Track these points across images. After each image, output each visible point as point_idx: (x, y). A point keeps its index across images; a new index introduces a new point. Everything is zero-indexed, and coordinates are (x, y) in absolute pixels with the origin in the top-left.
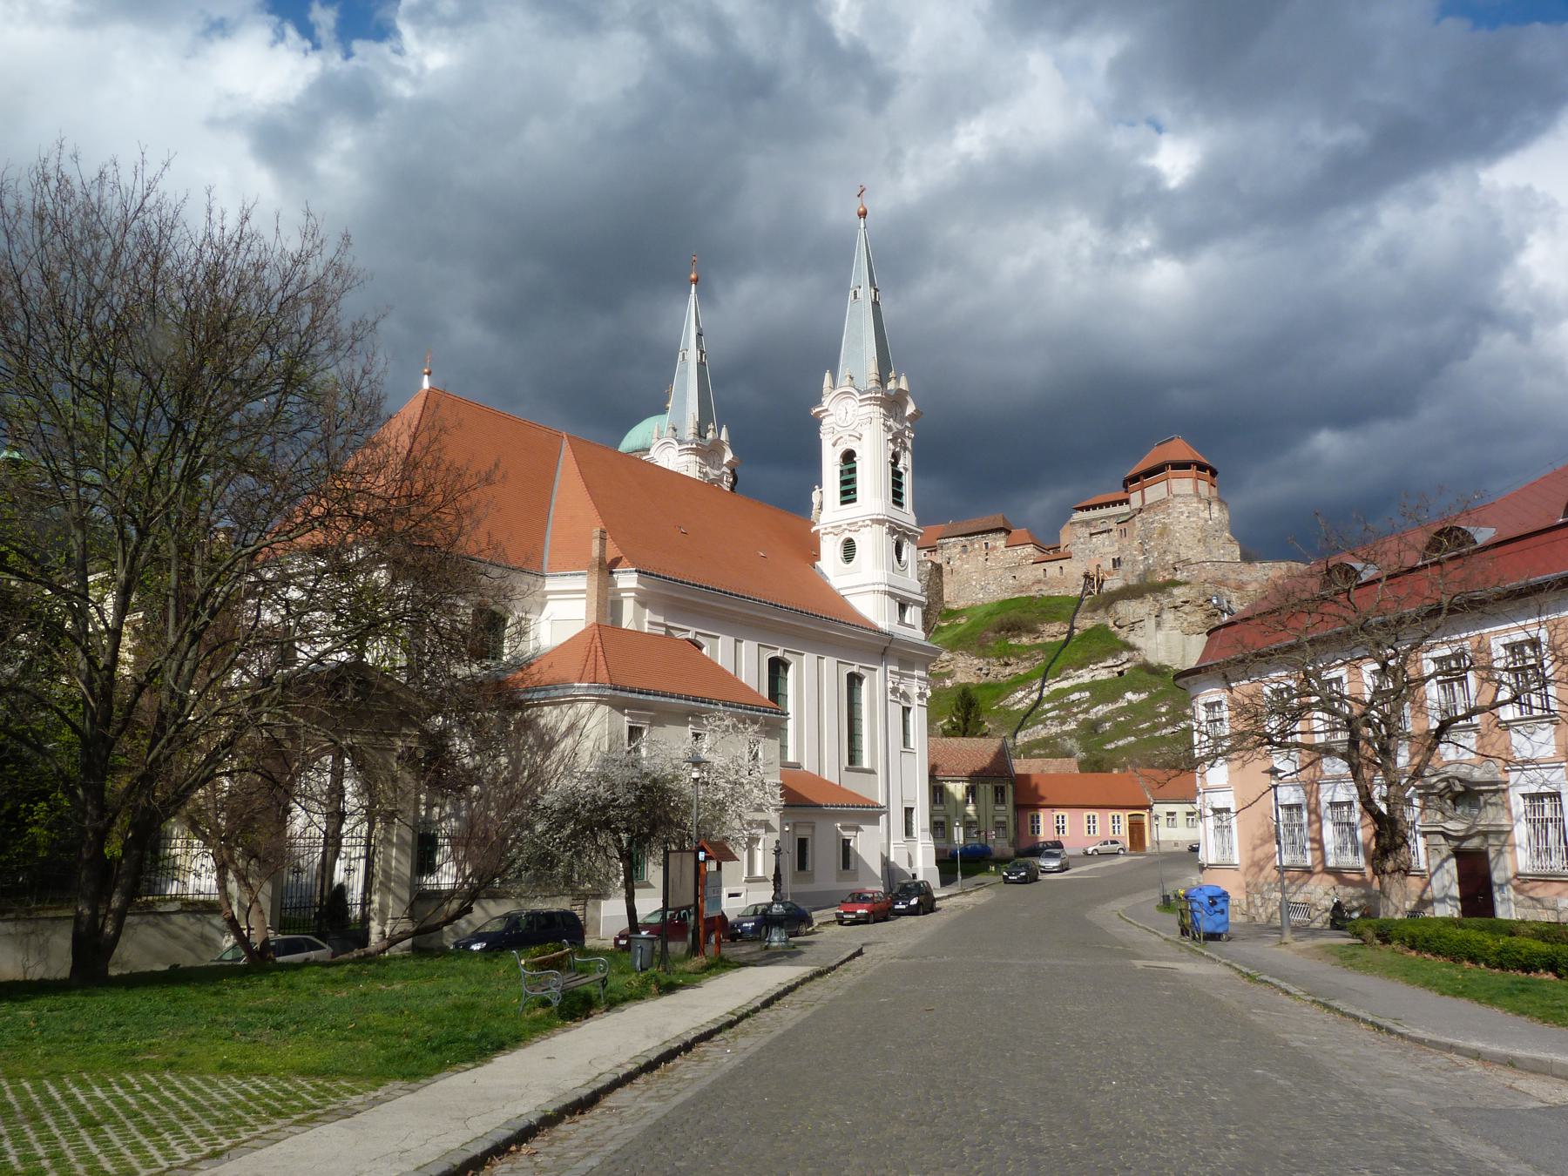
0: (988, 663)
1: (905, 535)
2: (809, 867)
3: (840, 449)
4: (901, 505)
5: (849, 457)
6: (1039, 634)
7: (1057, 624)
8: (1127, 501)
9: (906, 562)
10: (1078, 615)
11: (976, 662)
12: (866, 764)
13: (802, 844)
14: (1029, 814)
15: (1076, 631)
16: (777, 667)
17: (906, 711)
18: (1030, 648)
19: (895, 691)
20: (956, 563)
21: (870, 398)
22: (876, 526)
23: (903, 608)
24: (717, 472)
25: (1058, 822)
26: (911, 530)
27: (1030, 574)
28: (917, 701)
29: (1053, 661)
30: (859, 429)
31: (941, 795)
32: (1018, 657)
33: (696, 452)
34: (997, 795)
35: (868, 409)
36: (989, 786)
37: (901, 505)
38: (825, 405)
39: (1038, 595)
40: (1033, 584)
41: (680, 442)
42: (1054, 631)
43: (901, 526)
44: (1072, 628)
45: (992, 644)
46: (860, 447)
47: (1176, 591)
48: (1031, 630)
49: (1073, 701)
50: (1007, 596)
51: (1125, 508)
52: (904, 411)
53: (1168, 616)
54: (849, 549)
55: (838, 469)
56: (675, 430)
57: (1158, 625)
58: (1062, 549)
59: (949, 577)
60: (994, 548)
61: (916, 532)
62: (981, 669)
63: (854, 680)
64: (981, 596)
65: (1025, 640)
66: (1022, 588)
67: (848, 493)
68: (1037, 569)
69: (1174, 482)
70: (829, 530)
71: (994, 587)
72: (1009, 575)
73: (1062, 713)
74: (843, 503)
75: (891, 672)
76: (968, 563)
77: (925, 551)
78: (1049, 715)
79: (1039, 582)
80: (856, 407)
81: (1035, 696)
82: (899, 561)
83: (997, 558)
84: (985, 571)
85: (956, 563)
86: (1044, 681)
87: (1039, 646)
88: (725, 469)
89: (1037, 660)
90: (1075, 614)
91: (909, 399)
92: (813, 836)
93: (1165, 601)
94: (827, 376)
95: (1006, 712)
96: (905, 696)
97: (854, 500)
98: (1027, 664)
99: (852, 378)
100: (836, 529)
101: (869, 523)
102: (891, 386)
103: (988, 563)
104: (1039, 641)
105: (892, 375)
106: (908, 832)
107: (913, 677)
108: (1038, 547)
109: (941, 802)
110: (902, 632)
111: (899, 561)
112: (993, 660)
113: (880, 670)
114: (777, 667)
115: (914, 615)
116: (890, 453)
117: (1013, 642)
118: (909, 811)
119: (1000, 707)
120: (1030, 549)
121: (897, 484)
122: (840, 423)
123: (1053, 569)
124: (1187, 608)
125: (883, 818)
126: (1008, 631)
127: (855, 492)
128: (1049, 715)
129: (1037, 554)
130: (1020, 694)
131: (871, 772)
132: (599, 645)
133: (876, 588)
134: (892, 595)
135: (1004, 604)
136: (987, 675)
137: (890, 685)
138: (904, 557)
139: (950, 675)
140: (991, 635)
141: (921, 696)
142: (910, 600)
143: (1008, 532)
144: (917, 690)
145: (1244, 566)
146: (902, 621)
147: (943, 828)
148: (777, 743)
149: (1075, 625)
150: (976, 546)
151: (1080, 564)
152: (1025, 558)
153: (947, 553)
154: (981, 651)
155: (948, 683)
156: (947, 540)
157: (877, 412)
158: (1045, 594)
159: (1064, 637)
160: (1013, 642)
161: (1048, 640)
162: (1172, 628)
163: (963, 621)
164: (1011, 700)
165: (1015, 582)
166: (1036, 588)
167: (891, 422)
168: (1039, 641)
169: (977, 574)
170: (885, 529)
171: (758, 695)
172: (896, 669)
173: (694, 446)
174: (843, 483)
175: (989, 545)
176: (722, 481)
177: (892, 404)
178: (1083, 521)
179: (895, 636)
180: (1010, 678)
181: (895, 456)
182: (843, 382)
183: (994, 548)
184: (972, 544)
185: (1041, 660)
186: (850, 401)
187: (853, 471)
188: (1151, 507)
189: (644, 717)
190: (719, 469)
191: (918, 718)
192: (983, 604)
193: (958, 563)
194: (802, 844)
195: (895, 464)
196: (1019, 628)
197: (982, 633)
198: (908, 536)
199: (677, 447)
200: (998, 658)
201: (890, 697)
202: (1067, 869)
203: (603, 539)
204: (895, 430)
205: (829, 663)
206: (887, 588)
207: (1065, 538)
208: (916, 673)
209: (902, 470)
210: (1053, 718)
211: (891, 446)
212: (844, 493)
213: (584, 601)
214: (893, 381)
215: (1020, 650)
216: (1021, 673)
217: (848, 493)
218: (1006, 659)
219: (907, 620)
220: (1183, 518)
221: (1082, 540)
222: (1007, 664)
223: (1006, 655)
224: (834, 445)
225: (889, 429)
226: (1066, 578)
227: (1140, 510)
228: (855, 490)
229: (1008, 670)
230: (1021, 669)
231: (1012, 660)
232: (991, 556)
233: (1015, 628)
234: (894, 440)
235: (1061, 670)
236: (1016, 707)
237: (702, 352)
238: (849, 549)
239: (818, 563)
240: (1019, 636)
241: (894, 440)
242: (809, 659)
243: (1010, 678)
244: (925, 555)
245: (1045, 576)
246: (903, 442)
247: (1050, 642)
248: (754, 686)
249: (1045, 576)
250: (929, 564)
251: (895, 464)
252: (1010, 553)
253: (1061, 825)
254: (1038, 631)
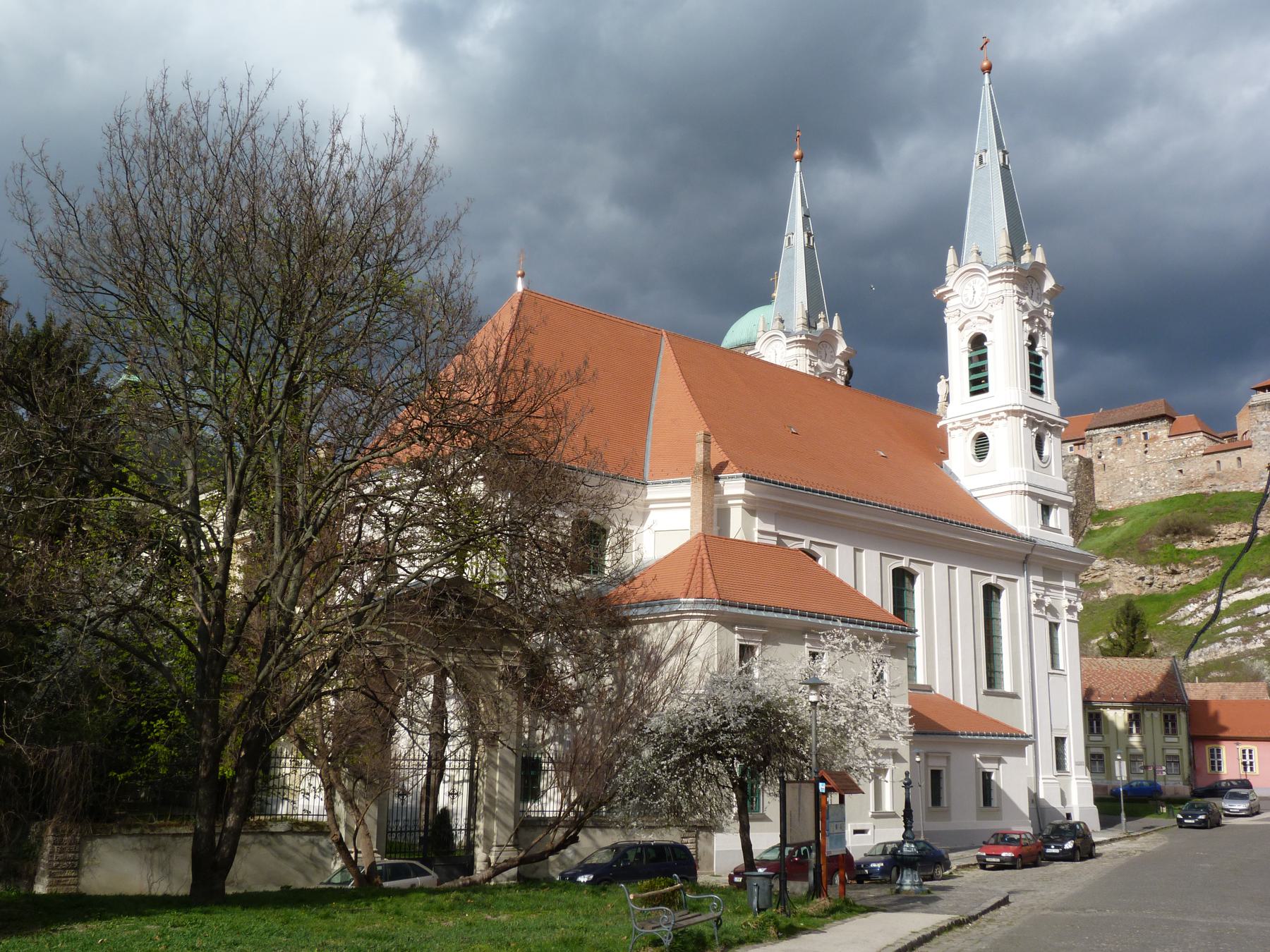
0: (1151, 571)
1: (1047, 427)
2: (944, 802)
4: (1040, 393)
5: (978, 342)
6: (1214, 536)
7: (1236, 524)
9: (1049, 458)
10: (1262, 514)
11: (1136, 570)
12: (1007, 687)
13: (936, 776)
14: (1208, 747)
15: (1261, 533)
16: (902, 579)
17: (1054, 627)
18: (1202, 553)
19: (1039, 604)
21: (1001, 275)
22: (1013, 418)
23: (1046, 509)
24: (829, 365)
25: (1244, 757)
26: (1054, 422)
27: (1199, 468)
28: (1066, 616)
29: (1233, 567)
30: (990, 311)
31: (1098, 724)
32: (1188, 563)
33: (806, 344)
34: (1166, 725)
35: (999, 287)
36: (1156, 714)
37: (1040, 393)
38: (950, 285)
39: (1211, 491)
40: (1205, 478)
41: (788, 334)
42: (1232, 533)
43: (1042, 418)
44: (1255, 529)
45: (1155, 549)
46: (991, 330)
48: (1203, 533)
49: (1259, 615)
50: (1172, 493)
52: (1041, 286)
54: (982, 444)
55: (966, 356)
56: (782, 321)
58: (1239, 437)
59: (1101, 473)
60: (1155, 438)
61: (1060, 423)
62: (1142, 579)
63: (991, 593)
64: (1140, 494)
65: (1197, 544)
66: (1191, 484)
67: (979, 383)
68: (1209, 461)
70: (958, 424)
71: (1156, 483)
72: (1173, 469)
73: (1246, 629)
74: (973, 393)
75: (1035, 583)
76: (1123, 457)
77: (1071, 445)
78: (1230, 631)
79: (1212, 476)
80: (985, 286)
81: (1211, 609)
82: (1040, 456)
83: (1160, 449)
84: (1145, 465)
85: (1108, 457)
86: (1221, 591)
87: (1214, 550)
88: (838, 362)
89: (1212, 567)
90: (1258, 512)
91: (1047, 273)
92: (948, 767)
94: (951, 254)
95: (1176, 627)
96: (1051, 610)
97: (986, 390)
98: (1199, 572)
99: (979, 253)
100: (966, 423)
101: (1004, 415)
102: (1025, 259)
103: (1148, 456)
104: (1214, 545)
105: (1026, 246)
106: (1060, 765)
107: (1060, 588)
108: (1210, 435)
109: (1099, 731)
110: (1046, 537)
111: (1040, 456)
112: (1157, 568)
113: (1022, 581)
114: (902, 579)
115: (1059, 518)
116: (1026, 336)
117: (1181, 546)
118: (1060, 741)
119: (1170, 622)
120: (1199, 438)
122: (967, 304)
123: (1229, 460)
125: (1029, 749)
126: (1176, 533)
127: (987, 381)
128: (1230, 631)
129: (1209, 443)
130: (1192, 607)
131: (1014, 696)
132: (705, 556)
133: (1014, 488)
134: (1033, 495)
135: (1170, 501)
136: (1151, 585)
137: (1034, 597)
138: (1046, 453)
139: (1105, 585)
140: (1154, 538)
141: (1071, 609)
142: (1054, 500)
143: (1172, 419)
144: (1065, 603)
146: (1045, 525)
147: (1102, 762)
148: (905, 663)
149: (1258, 526)
150: (1133, 437)
151: (1263, 454)
152: (1194, 449)
153: (1097, 446)
154: (1143, 558)
155: (1104, 595)
156: (1097, 431)
157: (1010, 289)
158: (1220, 490)
159: (1245, 540)
160: (1181, 546)
161: (1225, 543)
163: (1119, 523)
164: (1181, 614)
165: (1182, 477)
166: (1208, 483)
167: (1026, 300)
168: (1214, 545)
169: (1134, 469)
170: (1022, 422)
171: (881, 609)
172: (1040, 579)
173: (804, 338)
174: (973, 371)
175: (1149, 436)
176: (834, 374)
177: (1027, 280)
178: (1266, 403)
179: (1039, 542)
180: (1179, 588)
181: (1033, 339)
182: (969, 258)
183: (1155, 438)
184: (1128, 435)
185: (1217, 567)
186: (978, 279)
187: (983, 357)
189: (756, 634)
190: (831, 361)
191: (1068, 636)
192: (1144, 504)
193: (1111, 457)
194: (936, 776)
195: (1032, 347)
196: (1189, 531)
197: (1143, 537)
198: (1050, 429)
199: (785, 340)
200: (1164, 565)
201: (1034, 611)
202: (1258, 813)
203: (707, 442)
204: (1031, 309)
205: (962, 573)
206: (1027, 488)
207: (1242, 424)
208: (1064, 583)
209: (1041, 354)
210: (1234, 635)
211: (1027, 327)
212: (974, 383)
213: (688, 511)
214: (1027, 254)
215: (1190, 556)
216: (1193, 583)
217: (979, 383)
218: (1173, 567)
219: (1052, 523)
221: (1264, 425)
222: (1174, 573)
223: (1173, 562)
224: (961, 329)
225: (1025, 308)
226: (1245, 471)
228: (986, 379)
229: (1176, 579)
230: (1193, 577)
231: (1181, 567)
232: (1151, 448)
233: (1183, 530)
234: (1030, 321)
235: (1244, 577)
236: (1188, 622)
237: (809, 235)
238: (982, 444)
239: (945, 462)
240: (1189, 539)
241: (1030, 321)
242: (938, 570)
243: (1179, 588)
244: (1071, 449)
245: (1219, 468)
246: (1041, 322)
247: (1228, 547)
248: (877, 600)
249: (1219, 468)
250: (1077, 460)
251: (1032, 347)
252: (1174, 443)
253: (1248, 760)
254: (1212, 534)
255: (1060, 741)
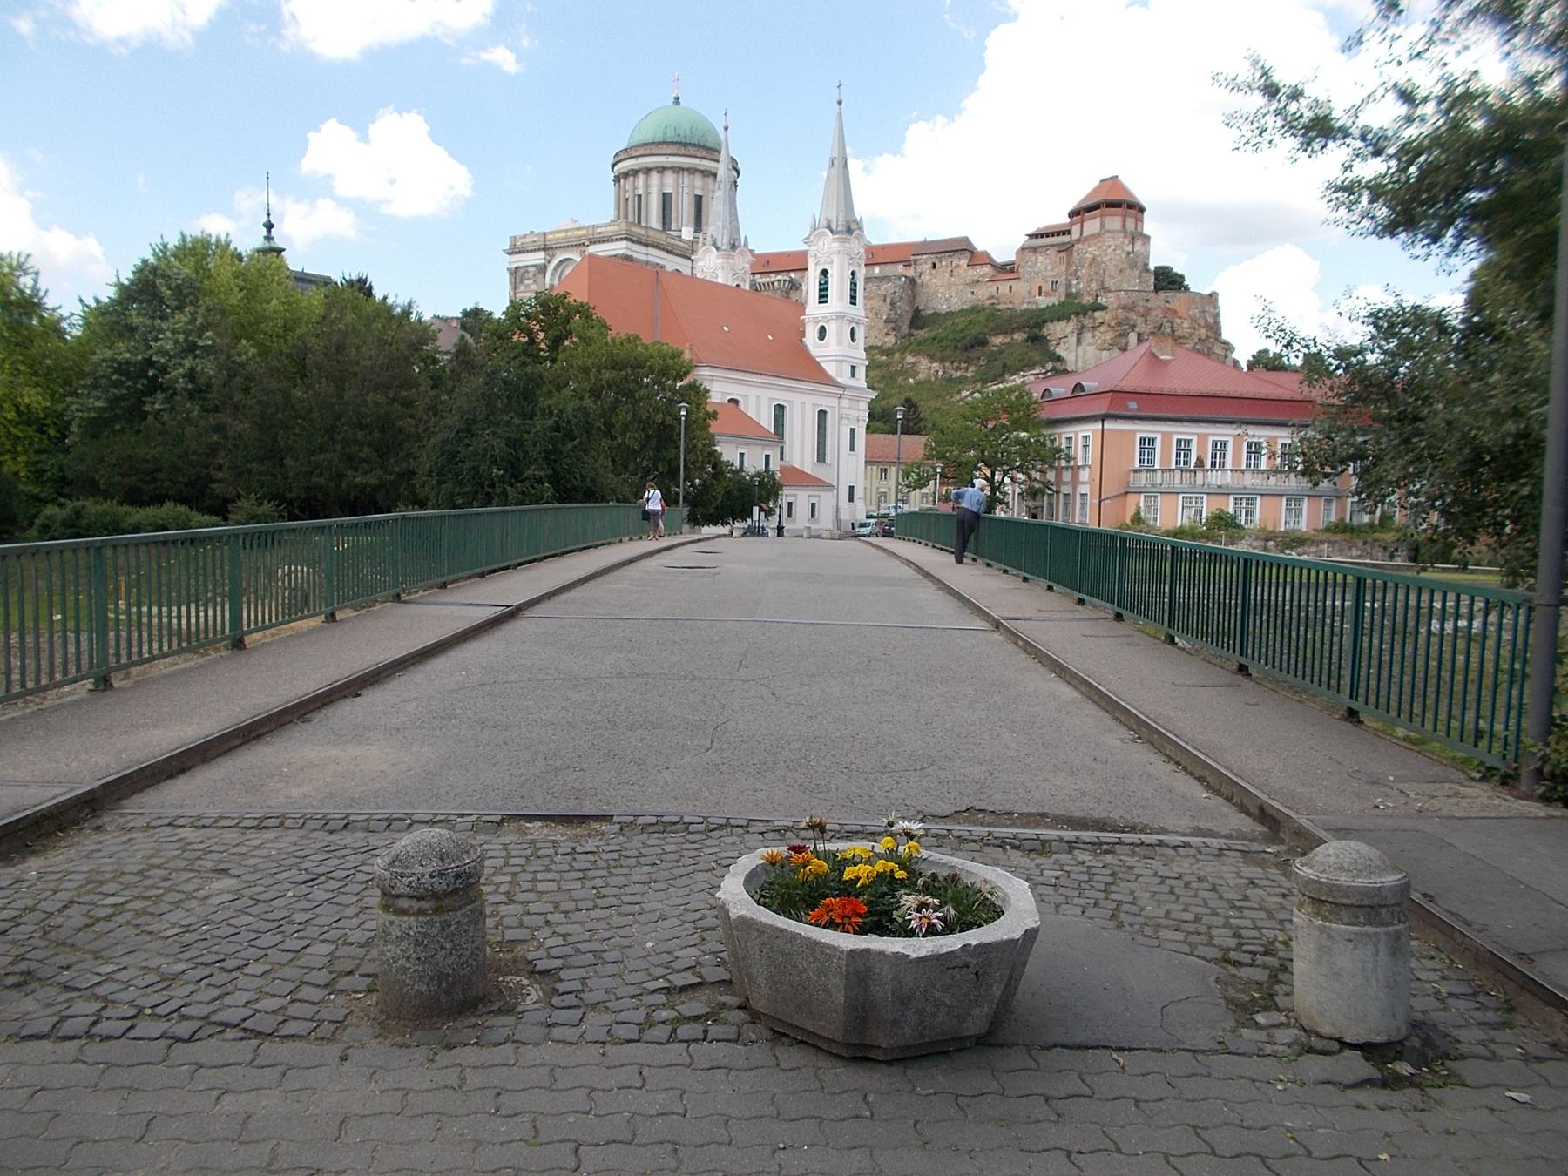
3: (820, 268)
5: (825, 273)
8: (1069, 232)
20: (926, 278)
47: (1097, 314)
51: (1066, 238)
53: (1087, 336)
54: (822, 333)
57: (1079, 342)
60: (958, 266)
67: (823, 298)
69: (1108, 220)
72: (969, 290)
79: (993, 297)
85: (926, 278)
93: (1088, 322)
115: (861, 372)
121: (854, 290)
123: (1004, 288)
124: (1102, 329)
145: (1152, 296)
152: (983, 276)
162: (1089, 344)
187: (827, 283)
188: (1087, 239)
193: (928, 277)
212: (820, 297)
217: (823, 298)
220: (1110, 250)
227: (1078, 241)
238: (822, 333)
252: (971, 272)
255: (852, 488)
